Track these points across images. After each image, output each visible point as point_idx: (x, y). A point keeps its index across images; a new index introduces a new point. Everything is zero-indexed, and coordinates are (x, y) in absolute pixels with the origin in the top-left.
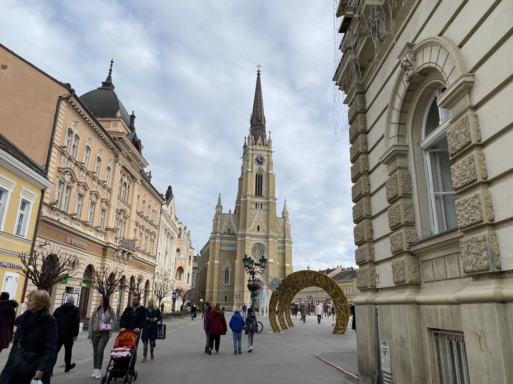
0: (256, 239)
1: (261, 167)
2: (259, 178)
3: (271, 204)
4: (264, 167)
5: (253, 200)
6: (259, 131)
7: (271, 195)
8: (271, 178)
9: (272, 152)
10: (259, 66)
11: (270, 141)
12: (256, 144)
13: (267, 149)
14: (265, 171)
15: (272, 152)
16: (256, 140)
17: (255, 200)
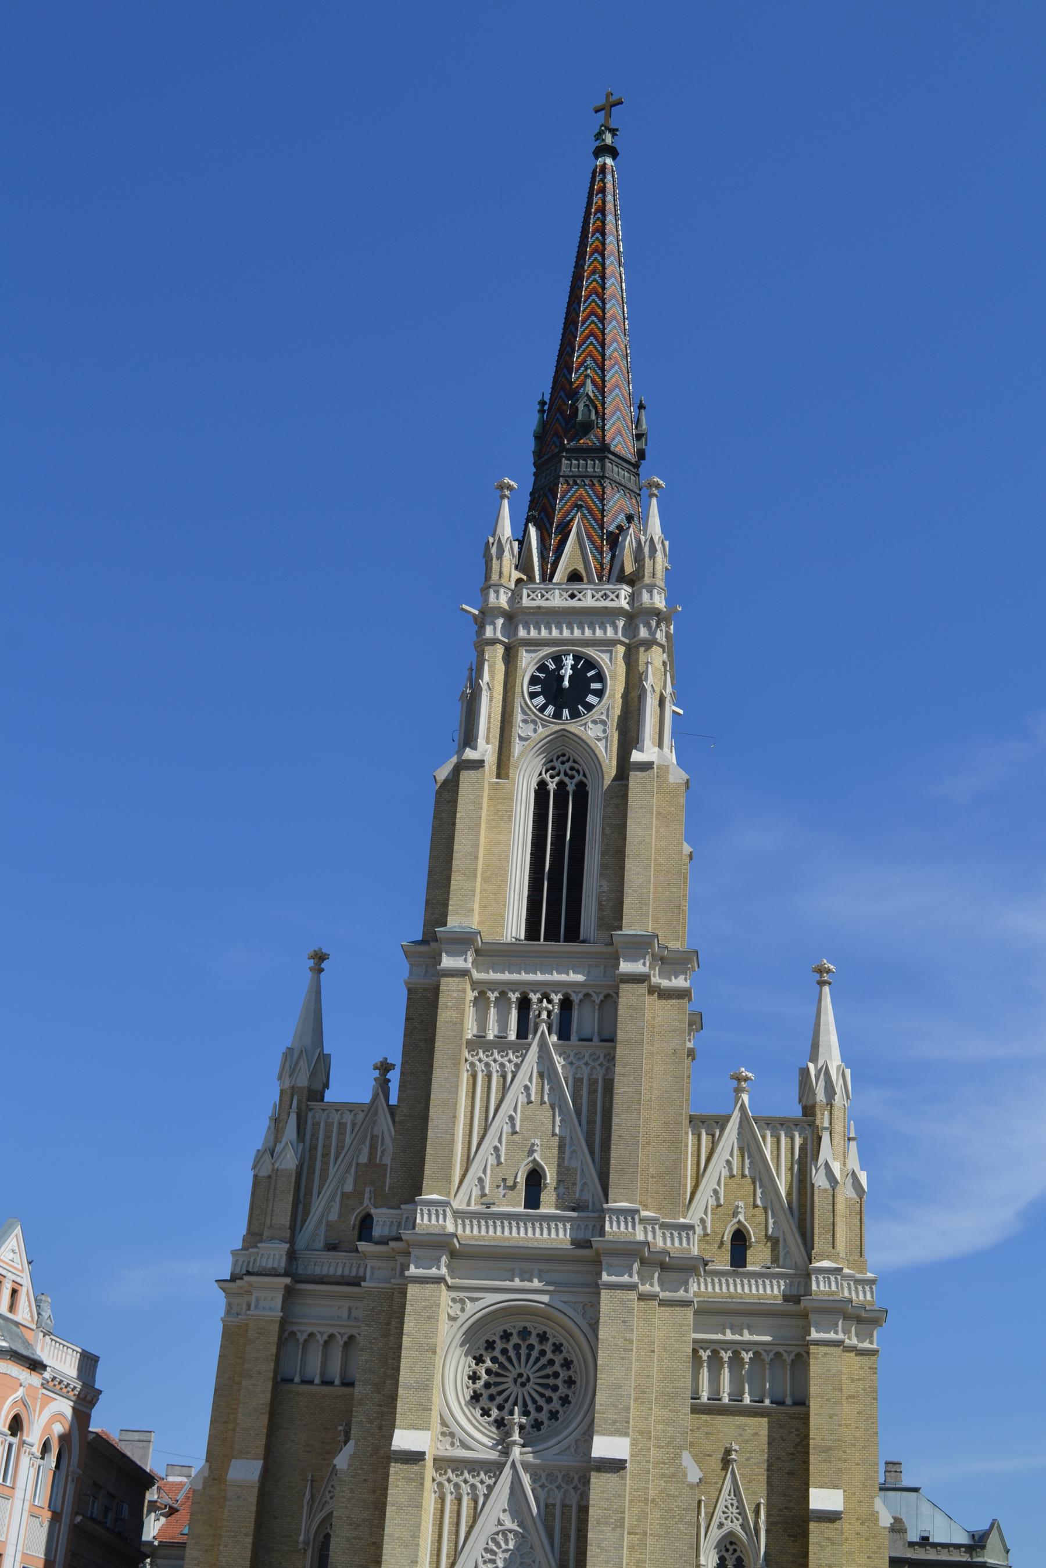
1: (574, 727)
3: (628, 995)
4: (596, 731)
7: (632, 926)
10: (610, 105)
12: (547, 577)
16: (551, 554)
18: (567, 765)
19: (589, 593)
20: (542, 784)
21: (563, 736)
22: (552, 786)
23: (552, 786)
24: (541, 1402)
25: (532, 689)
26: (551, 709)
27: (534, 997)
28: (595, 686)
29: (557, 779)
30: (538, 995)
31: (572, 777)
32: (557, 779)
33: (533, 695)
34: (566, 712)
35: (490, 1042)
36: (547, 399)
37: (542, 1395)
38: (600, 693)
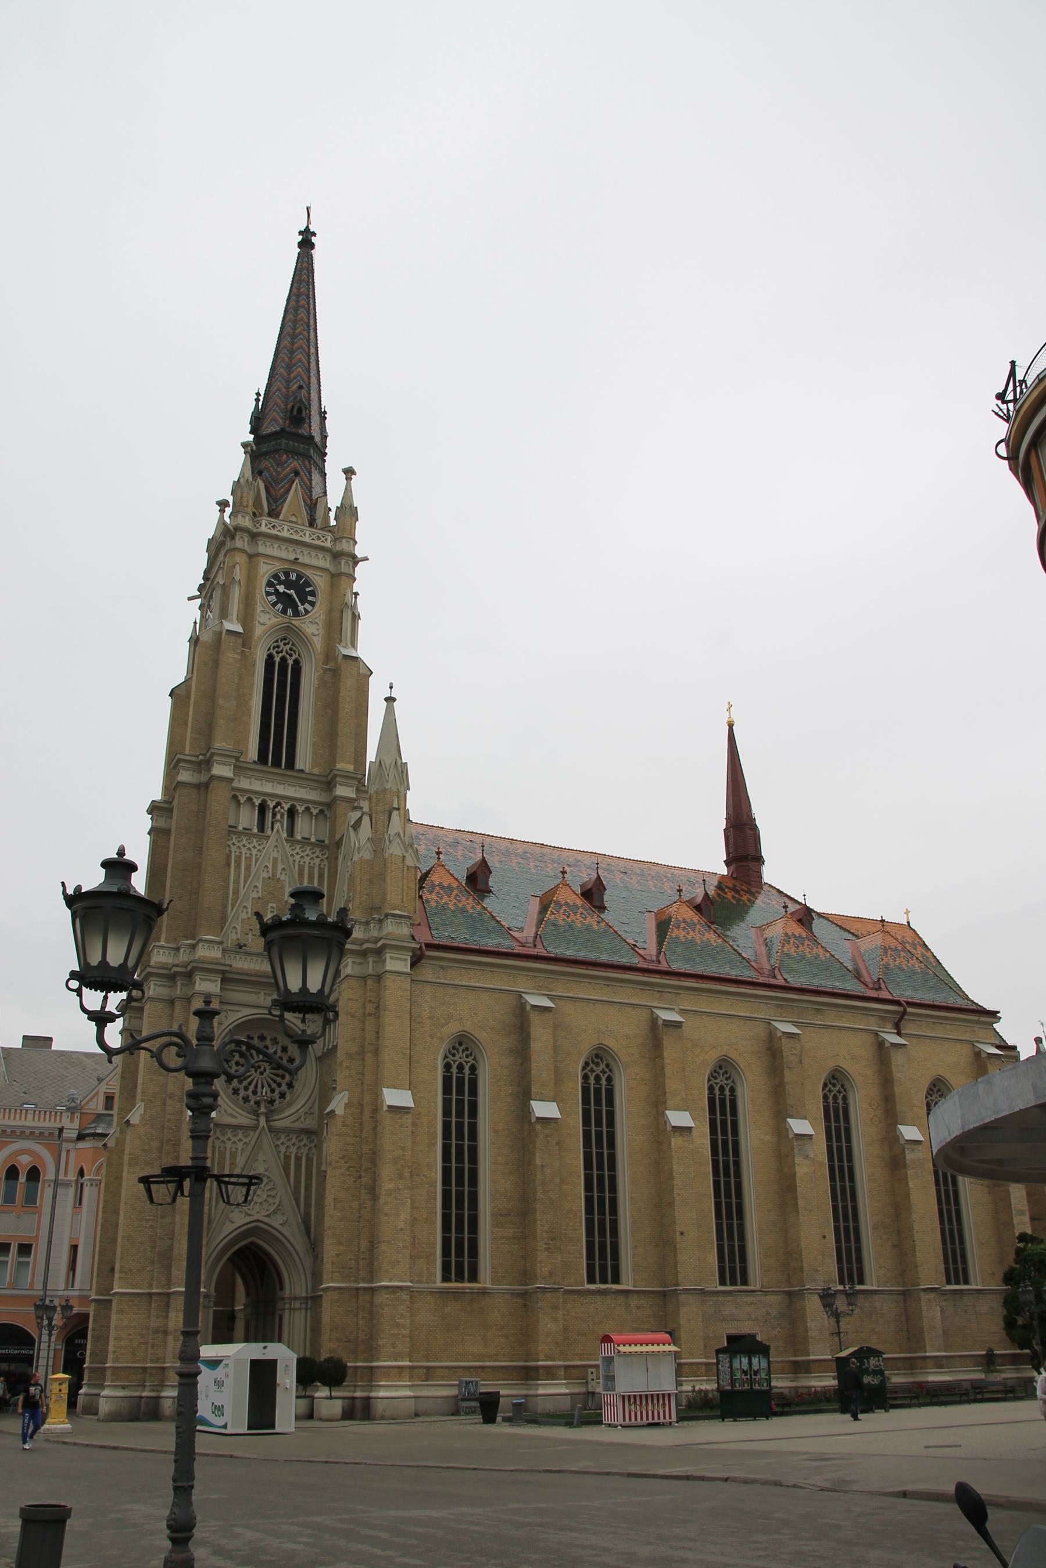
0: (251, 998)
1: (296, 622)
2: (282, 680)
4: (312, 625)
5: (244, 783)
6: (294, 464)
8: (348, 683)
9: (355, 561)
11: (348, 511)
12: (274, 513)
13: (328, 544)
14: (318, 643)
15: (355, 561)
17: (256, 786)
18: (288, 647)
19: (308, 533)
20: (270, 657)
21: (289, 628)
22: (277, 659)
23: (277, 659)
24: (274, 1085)
25: (268, 589)
26: (280, 606)
27: (271, 804)
28: (309, 598)
29: (281, 655)
30: (274, 803)
31: (291, 655)
32: (281, 655)
33: (268, 594)
34: (290, 611)
35: (240, 833)
36: (262, 393)
37: (275, 1081)
38: (313, 604)
